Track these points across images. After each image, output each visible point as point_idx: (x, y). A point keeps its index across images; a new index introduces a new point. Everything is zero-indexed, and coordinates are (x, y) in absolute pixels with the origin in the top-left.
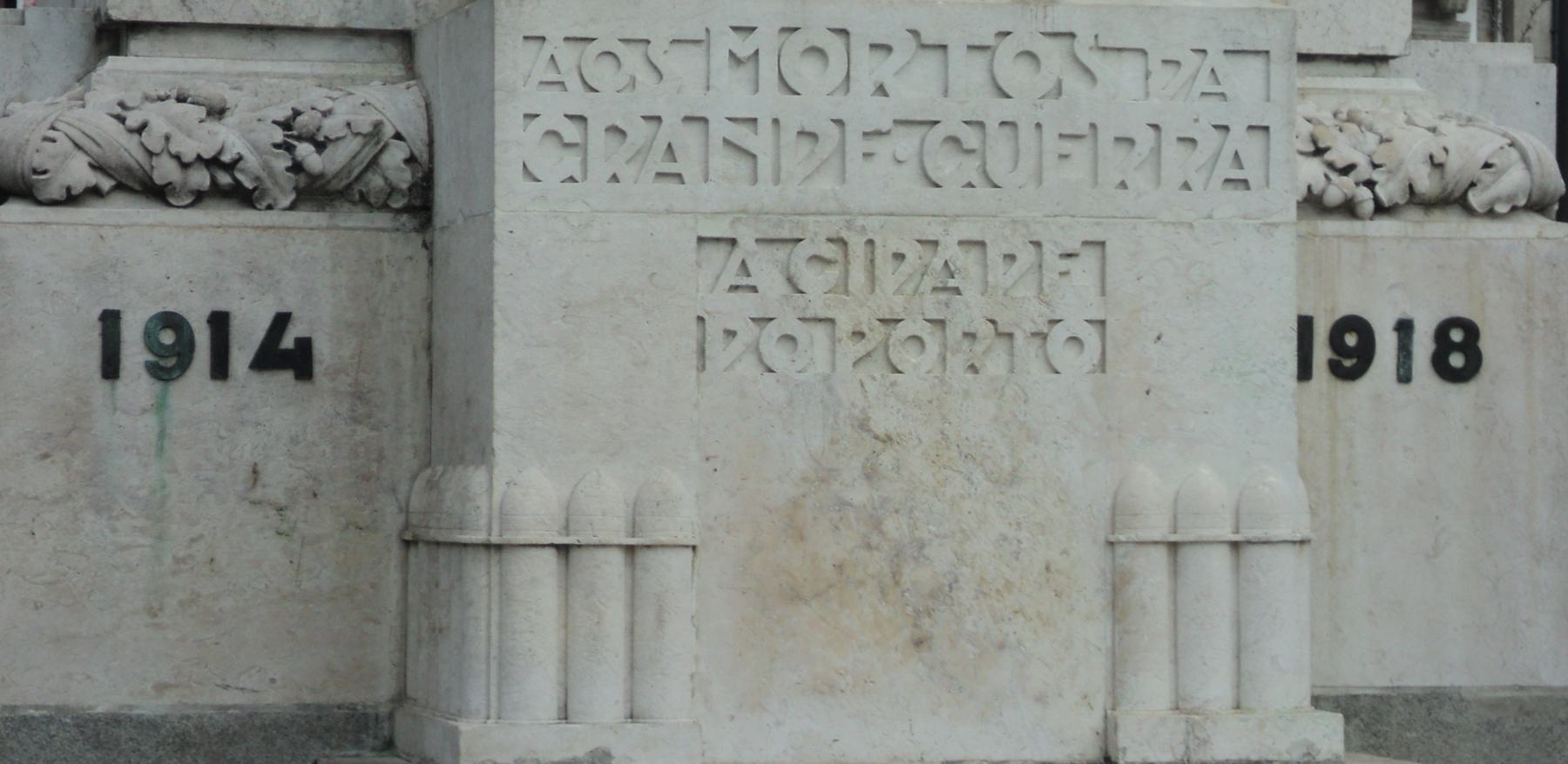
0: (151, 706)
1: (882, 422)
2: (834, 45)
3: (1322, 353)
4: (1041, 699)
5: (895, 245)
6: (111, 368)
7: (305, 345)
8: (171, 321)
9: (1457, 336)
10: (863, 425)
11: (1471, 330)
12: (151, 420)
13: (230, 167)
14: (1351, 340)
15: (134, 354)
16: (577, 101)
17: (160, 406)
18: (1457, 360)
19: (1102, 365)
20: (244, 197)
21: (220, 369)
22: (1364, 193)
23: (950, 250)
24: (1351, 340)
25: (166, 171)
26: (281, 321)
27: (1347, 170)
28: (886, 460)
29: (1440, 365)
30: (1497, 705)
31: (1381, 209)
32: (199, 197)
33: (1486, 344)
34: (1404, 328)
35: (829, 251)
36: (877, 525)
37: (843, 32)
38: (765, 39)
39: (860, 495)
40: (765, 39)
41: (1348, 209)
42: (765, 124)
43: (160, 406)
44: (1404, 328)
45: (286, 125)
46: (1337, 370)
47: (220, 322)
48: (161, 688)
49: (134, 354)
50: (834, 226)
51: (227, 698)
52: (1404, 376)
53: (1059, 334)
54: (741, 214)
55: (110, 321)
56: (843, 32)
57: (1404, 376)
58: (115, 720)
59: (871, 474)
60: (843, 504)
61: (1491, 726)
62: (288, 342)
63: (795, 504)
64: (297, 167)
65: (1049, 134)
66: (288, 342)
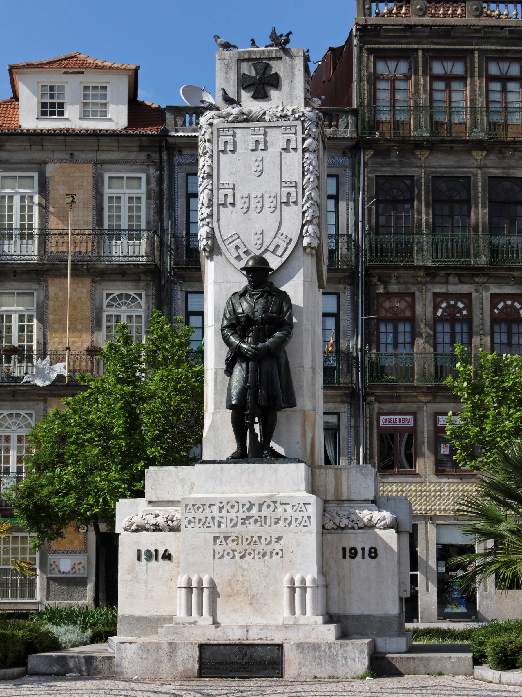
0: (145, 615)
1: (245, 566)
2: (236, 504)
3: (348, 554)
4: (272, 613)
5: (247, 537)
6: (139, 559)
7: (170, 555)
8: (148, 551)
9: (373, 550)
10: (242, 568)
11: (376, 550)
12: (145, 567)
13: (158, 525)
14: (353, 551)
15: (143, 556)
16: (193, 514)
17: (147, 565)
18: (373, 555)
19: (282, 557)
20: (161, 530)
21: (156, 559)
22: (356, 525)
23: (256, 538)
24: (353, 551)
25: (147, 526)
26: (166, 551)
27: (353, 521)
28: (245, 572)
29: (370, 556)
30: (381, 617)
31: (359, 528)
32: (154, 531)
33: (379, 552)
34: (363, 549)
35: (236, 538)
36: (244, 584)
37: (238, 502)
38: (224, 504)
39: (241, 579)
40: (224, 504)
41: (353, 528)
42: (225, 518)
43: (147, 565)
44: (363, 549)
45: (167, 518)
46: (351, 557)
47: (156, 551)
48: (147, 612)
49: (143, 556)
50: (237, 534)
51: (158, 614)
52: (363, 557)
53: (275, 552)
54: (221, 533)
55: (139, 551)
56: (238, 502)
57: (363, 557)
58: (140, 617)
59: (243, 575)
60: (238, 580)
61: (380, 621)
62: (167, 554)
63: (230, 580)
64: (169, 525)
65: (273, 518)
66: (167, 554)
